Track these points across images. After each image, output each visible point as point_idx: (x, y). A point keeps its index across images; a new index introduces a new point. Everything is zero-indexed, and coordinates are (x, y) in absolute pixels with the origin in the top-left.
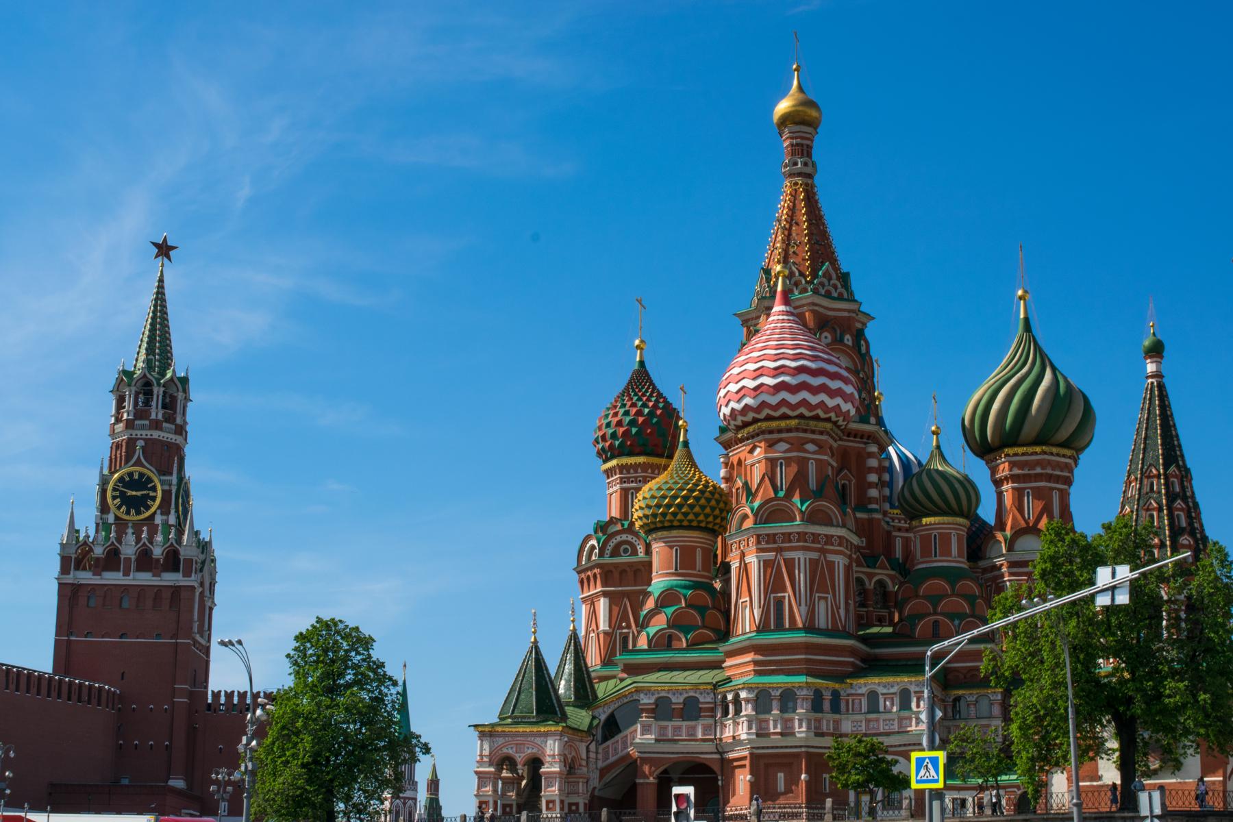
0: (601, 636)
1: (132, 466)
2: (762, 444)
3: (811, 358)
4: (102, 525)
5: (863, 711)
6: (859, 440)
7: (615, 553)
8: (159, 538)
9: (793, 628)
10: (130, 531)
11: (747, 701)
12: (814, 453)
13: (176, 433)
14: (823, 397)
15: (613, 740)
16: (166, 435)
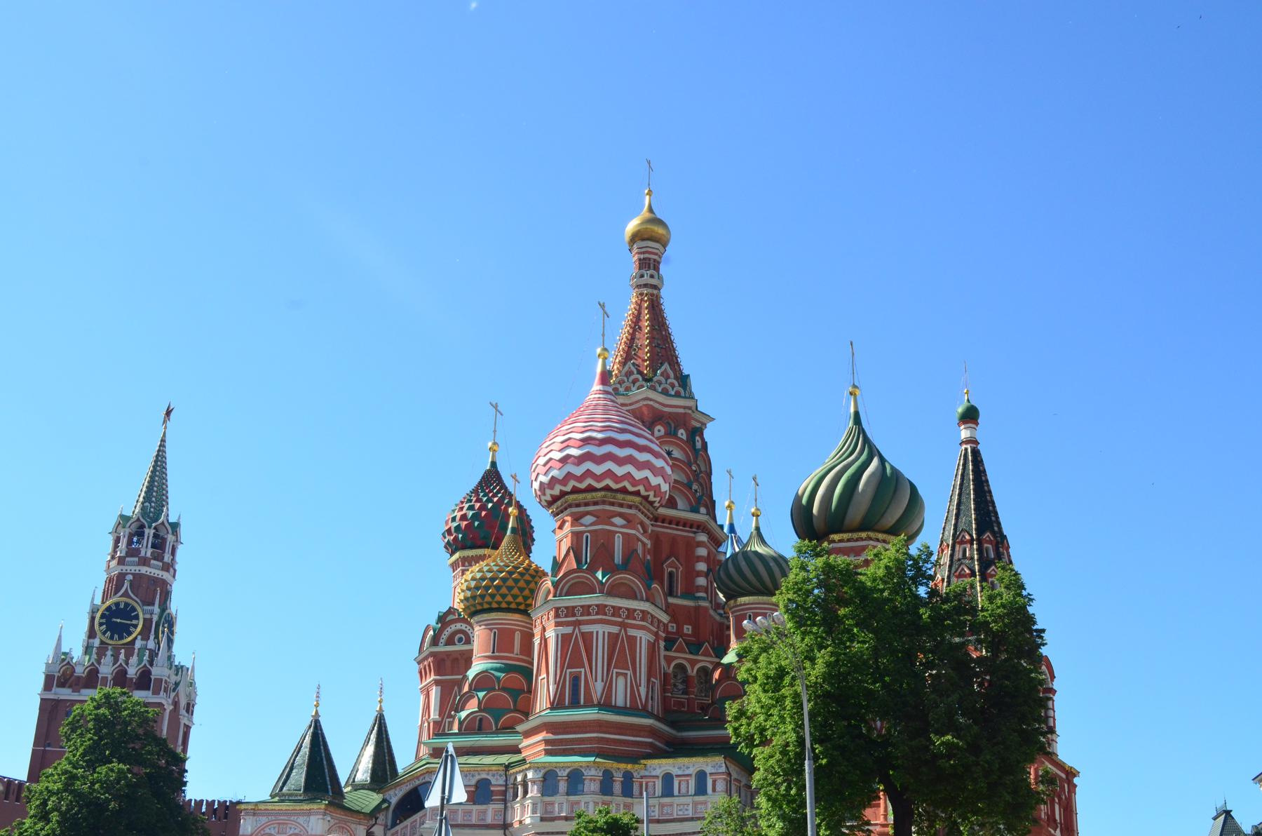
0: (431, 724)
1: (120, 597)
2: (569, 518)
3: (619, 431)
4: (88, 649)
5: (657, 795)
6: (688, 529)
7: (450, 641)
8: (134, 660)
9: (589, 704)
10: (109, 653)
11: (534, 782)
12: (622, 527)
13: (162, 570)
14: (629, 468)
15: (402, 825)
16: (153, 571)
